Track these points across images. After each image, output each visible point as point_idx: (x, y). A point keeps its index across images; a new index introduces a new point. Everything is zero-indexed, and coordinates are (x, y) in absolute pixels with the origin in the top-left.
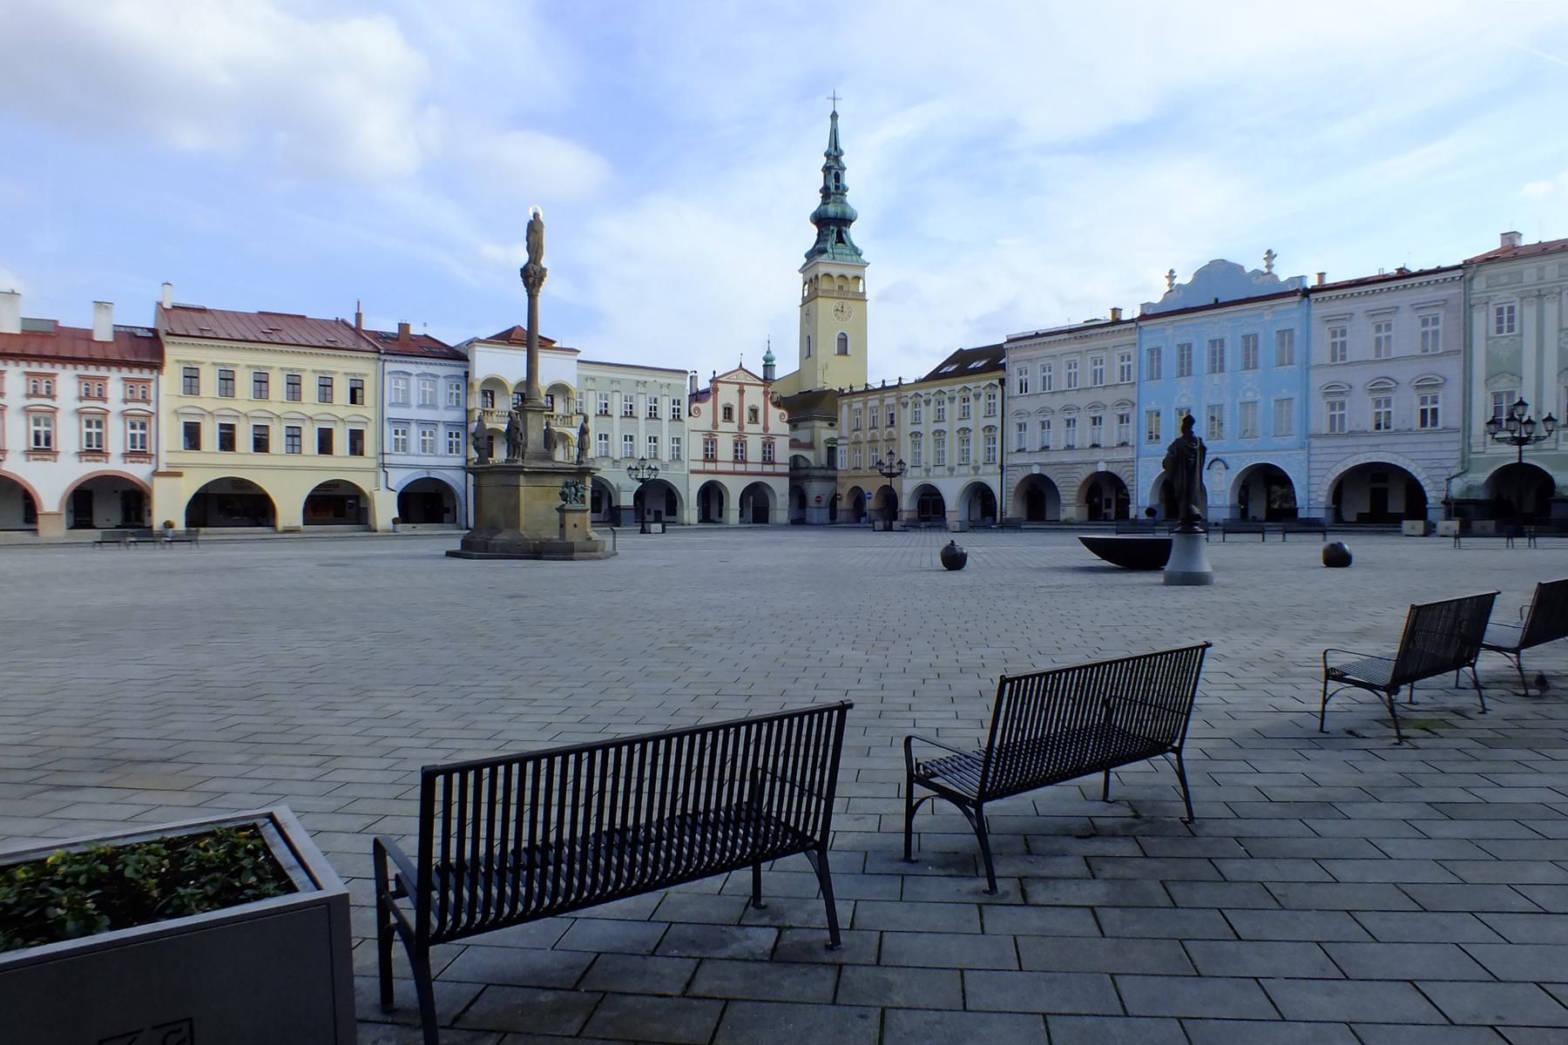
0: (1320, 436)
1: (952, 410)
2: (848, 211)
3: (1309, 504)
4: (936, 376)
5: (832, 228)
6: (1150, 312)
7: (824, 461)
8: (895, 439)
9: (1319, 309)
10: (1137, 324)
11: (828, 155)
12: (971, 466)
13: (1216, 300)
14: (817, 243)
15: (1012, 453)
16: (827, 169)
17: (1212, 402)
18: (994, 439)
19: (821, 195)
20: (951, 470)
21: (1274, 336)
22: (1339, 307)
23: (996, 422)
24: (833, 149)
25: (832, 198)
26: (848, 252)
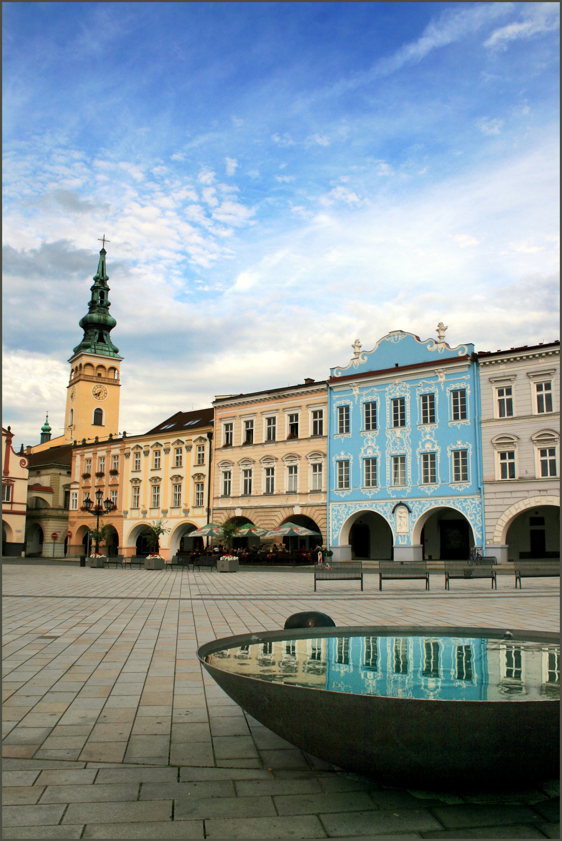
0: (493, 483)
1: (168, 460)
2: (109, 319)
3: (486, 544)
4: (156, 431)
5: (96, 330)
6: (340, 375)
7: (61, 503)
8: (117, 485)
9: (485, 373)
10: (328, 385)
11: (96, 279)
12: (182, 509)
13: (397, 365)
14: (84, 340)
15: (218, 498)
16: (94, 289)
17: (394, 453)
18: (203, 485)
20: (165, 512)
21: (448, 395)
22: (502, 370)
23: (204, 470)
25: (97, 309)
26: (107, 349)
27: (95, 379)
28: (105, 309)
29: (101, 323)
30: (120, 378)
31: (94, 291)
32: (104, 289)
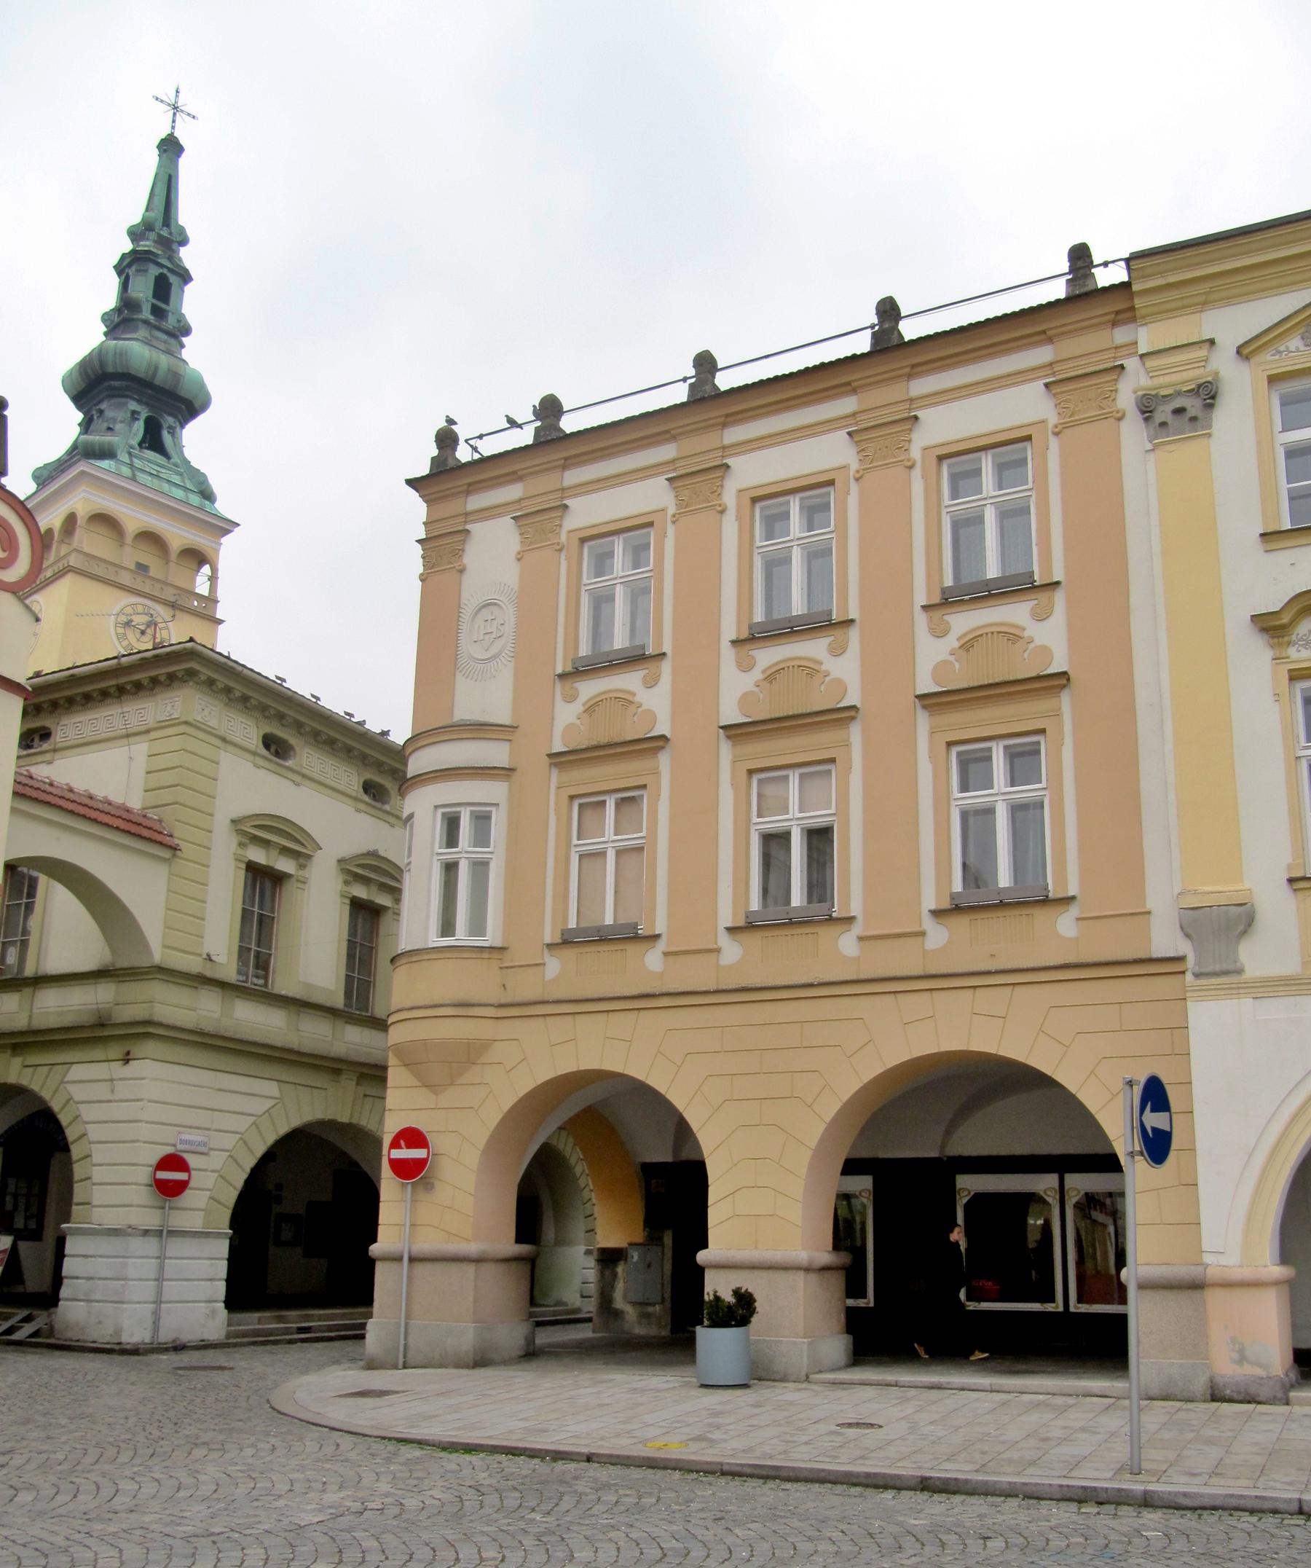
5: (133, 405)
19: (105, 329)
24: (157, 214)
26: (176, 479)
27: (125, 578)
28: (172, 341)
29: (157, 382)
30: (221, 594)
31: (131, 271)
32: (170, 270)
